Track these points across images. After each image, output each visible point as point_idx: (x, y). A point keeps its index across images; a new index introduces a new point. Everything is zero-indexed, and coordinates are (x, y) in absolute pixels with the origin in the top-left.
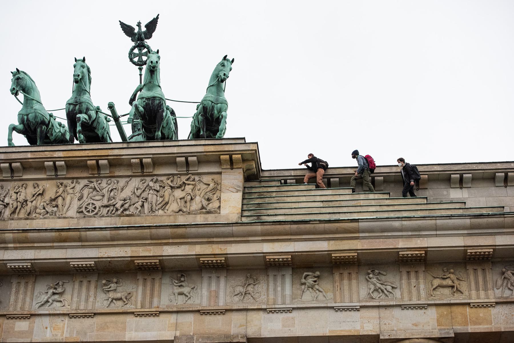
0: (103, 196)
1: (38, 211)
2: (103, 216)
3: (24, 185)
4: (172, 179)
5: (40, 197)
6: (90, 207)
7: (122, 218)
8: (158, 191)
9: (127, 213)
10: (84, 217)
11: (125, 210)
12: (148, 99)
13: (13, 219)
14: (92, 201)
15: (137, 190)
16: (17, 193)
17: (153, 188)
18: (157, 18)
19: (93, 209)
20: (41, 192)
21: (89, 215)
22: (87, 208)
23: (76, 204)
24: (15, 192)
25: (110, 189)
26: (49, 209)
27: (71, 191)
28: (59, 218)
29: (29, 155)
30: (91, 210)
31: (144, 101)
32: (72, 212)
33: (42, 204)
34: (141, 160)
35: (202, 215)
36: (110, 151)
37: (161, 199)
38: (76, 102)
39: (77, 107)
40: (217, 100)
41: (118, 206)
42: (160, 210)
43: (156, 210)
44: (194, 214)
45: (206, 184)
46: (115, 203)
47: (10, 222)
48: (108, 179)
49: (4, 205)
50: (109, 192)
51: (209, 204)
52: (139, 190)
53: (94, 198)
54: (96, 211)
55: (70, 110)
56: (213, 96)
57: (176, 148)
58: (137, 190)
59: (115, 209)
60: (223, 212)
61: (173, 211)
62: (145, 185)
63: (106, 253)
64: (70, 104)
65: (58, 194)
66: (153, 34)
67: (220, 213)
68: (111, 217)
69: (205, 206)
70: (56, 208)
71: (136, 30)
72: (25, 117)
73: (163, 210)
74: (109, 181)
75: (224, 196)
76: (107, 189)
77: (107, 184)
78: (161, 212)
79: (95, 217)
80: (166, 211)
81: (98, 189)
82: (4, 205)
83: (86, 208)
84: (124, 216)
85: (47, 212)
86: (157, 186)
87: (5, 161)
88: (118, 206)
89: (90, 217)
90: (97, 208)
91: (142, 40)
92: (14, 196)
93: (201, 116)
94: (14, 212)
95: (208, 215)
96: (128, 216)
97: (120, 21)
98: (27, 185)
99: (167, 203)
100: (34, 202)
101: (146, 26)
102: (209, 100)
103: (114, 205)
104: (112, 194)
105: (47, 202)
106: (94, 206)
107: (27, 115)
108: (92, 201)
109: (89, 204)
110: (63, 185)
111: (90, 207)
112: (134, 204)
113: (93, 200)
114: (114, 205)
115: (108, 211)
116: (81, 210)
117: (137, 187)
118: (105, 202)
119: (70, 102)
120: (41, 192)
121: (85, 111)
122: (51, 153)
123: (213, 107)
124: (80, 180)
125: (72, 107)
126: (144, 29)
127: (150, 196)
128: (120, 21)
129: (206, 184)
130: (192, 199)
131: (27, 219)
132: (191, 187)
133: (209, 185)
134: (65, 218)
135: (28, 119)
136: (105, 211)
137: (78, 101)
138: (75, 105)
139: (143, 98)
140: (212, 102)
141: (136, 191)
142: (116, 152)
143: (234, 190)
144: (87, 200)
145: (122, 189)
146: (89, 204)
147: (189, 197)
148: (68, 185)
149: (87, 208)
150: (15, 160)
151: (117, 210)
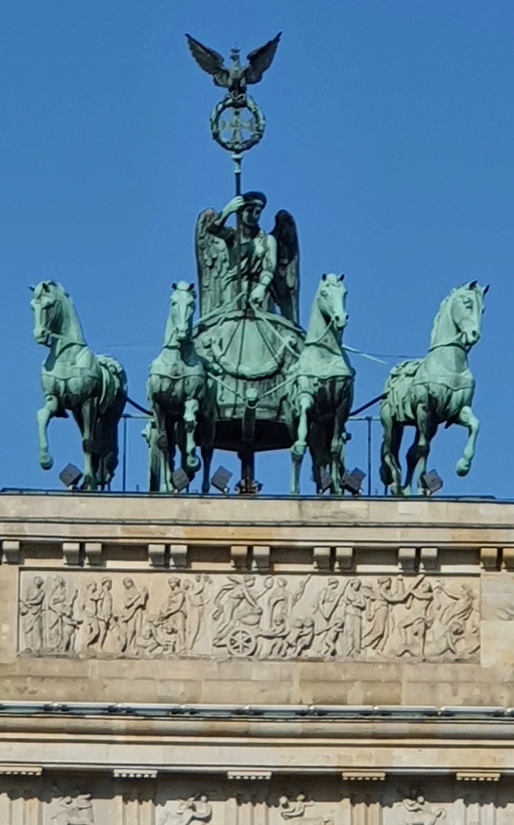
0: (261, 614)
1: (140, 641)
2: (265, 659)
3: (107, 584)
4: (388, 583)
5: (140, 610)
6: (240, 640)
7: (300, 664)
8: (363, 609)
9: (309, 653)
10: (230, 658)
11: (306, 647)
12: (322, 381)
13: (94, 657)
14: (243, 628)
15: (324, 602)
16: (96, 601)
17: (354, 604)
18: (277, 39)
19: (246, 644)
20: (141, 601)
21: (239, 655)
22: (236, 642)
23: (210, 630)
24: (92, 600)
25: (273, 601)
26: (162, 636)
27: (197, 600)
28: (183, 658)
29: (118, 531)
30: (241, 647)
31: (316, 385)
32: (205, 645)
33: (148, 627)
34: (333, 550)
35: (449, 665)
36: (274, 530)
37: (368, 627)
38: (177, 375)
39: (178, 387)
40: (457, 382)
41: (291, 638)
42: (369, 649)
43: (361, 648)
44: (433, 662)
45: (451, 597)
46: (284, 634)
47: (91, 662)
48: (265, 577)
49: (75, 627)
50: (271, 607)
51: (457, 640)
52: (326, 604)
53: (245, 620)
54: (252, 646)
55: (164, 389)
56: (449, 373)
57: (398, 531)
58: (324, 602)
59: (286, 645)
60: (487, 660)
61: (392, 651)
62: (338, 591)
63: (292, 758)
64: (162, 377)
65: (174, 607)
66: (265, 74)
67: (479, 663)
68: (280, 660)
69: (451, 646)
70: (173, 635)
71: (228, 65)
72: (62, 384)
73: (374, 648)
74: (269, 581)
75: (485, 628)
76: (266, 597)
77: (265, 586)
78: (370, 652)
79: (250, 660)
80: (379, 651)
81: (250, 600)
82: (75, 627)
83: (233, 642)
84: (304, 661)
85: (159, 645)
86: (360, 598)
87: (72, 540)
88: (291, 638)
89: (242, 659)
90: (253, 639)
91: (243, 90)
92: (90, 609)
93: (424, 408)
94: (95, 641)
95: (458, 665)
96: (311, 660)
97: (187, 35)
98: (111, 582)
99: (382, 636)
100: (131, 622)
101: (249, 58)
102: (443, 384)
103: (284, 637)
104: (278, 610)
105: (156, 623)
106: (245, 639)
107: (66, 380)
108: (243, 628)
109: (237, 632)
110: (181, 584)
111: (240, 640)
112: (319, 634)
113: (245, 623)
114: (284, 637)
115: (274, 646)
116: (222, 642)
117: (322, 597)
118: (265, 627)
119: (163, 373)
120: (143, 603)
121: (193, 393)
122: (162, 528)
123: (449, 398)
124: (212, 576)
125: (166, 385)
126: (245, 63)
127: (348, 617)
128: (187, 35)
129: (451, 597)
130: (427, 628)
131: (123, 658)
132: (425, 603)
133: (457, 599)
134: (193, 658)
135: (66, 388)
136: (265, 646)
137: (180, 372)
138: (174, 382)
139: (313, 377)
140: (448, 388)
141: (321, 606)
142: (286, 533)
143: (505, 616)
144: (232, 623)
145: (295, 600)
146: (237, 632)
147: (422, 626)
148: (191, 585)
149: (236, 642)
150: (93, 539)
151: (290, 646)
